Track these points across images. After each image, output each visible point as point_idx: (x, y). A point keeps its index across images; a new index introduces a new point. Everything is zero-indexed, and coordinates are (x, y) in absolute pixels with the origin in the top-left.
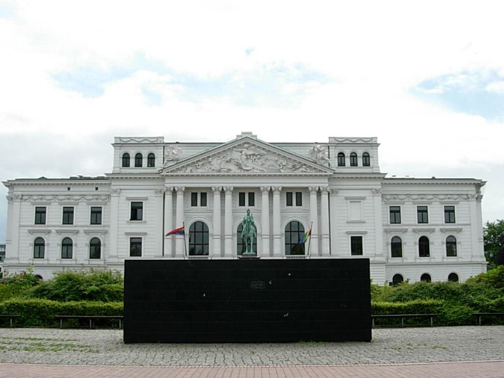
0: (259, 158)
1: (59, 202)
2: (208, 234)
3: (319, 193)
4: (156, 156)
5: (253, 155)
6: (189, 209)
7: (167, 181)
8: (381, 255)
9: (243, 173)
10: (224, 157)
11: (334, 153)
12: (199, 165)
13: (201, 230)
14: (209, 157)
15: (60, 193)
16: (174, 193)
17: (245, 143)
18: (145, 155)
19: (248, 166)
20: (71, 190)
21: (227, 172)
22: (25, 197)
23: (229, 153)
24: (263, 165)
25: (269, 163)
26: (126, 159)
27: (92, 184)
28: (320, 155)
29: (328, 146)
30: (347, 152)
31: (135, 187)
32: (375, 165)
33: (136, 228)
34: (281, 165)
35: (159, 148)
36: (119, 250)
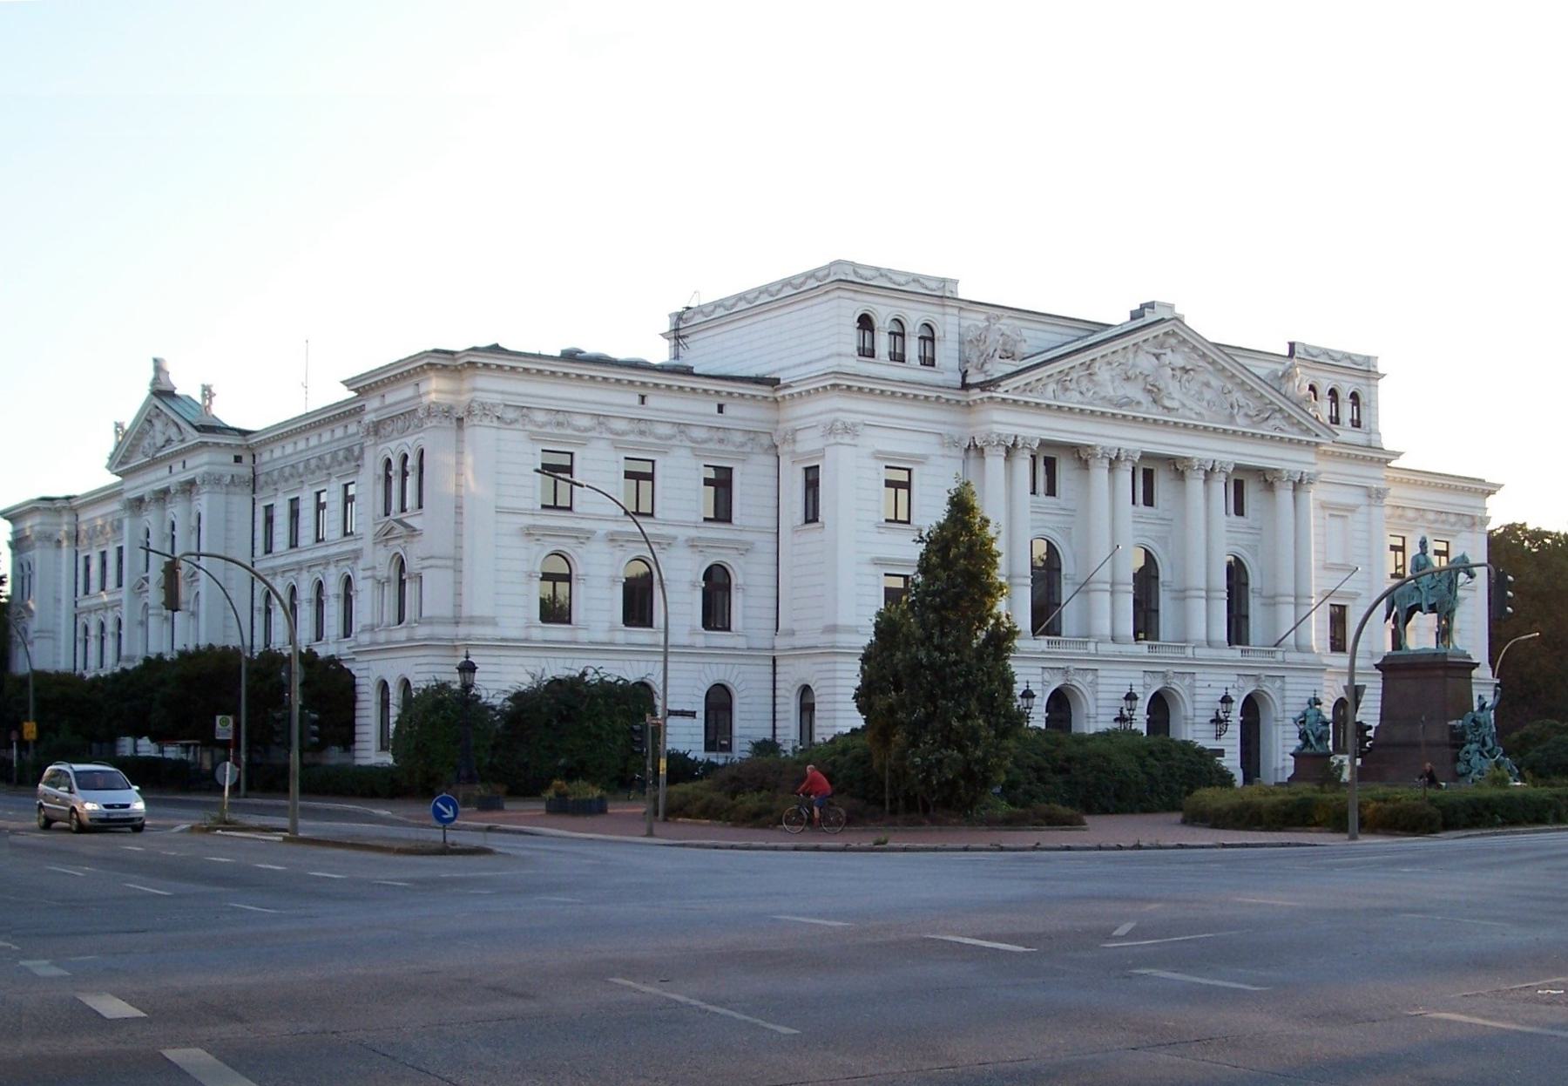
1: (613, 441)
9: (1156, 413)
18: (913, 329)
20: (650, 401)
35: (949, 310)
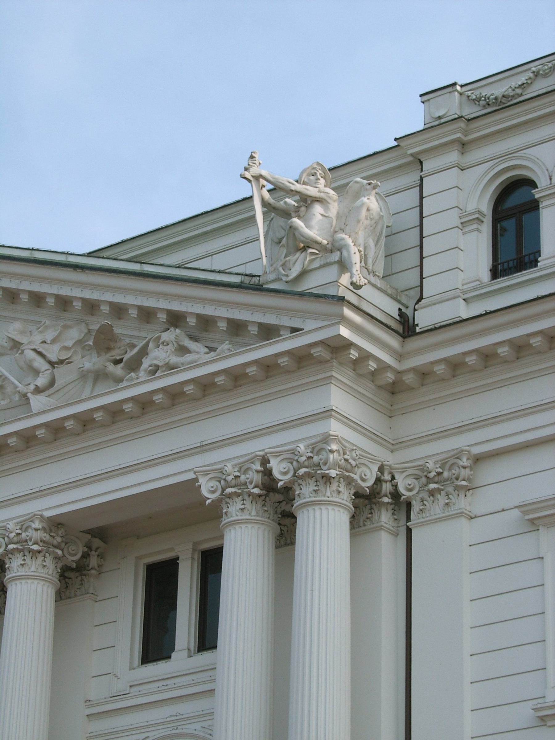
11: (461, 192)
29: (406, 159)
34: (40, 363)
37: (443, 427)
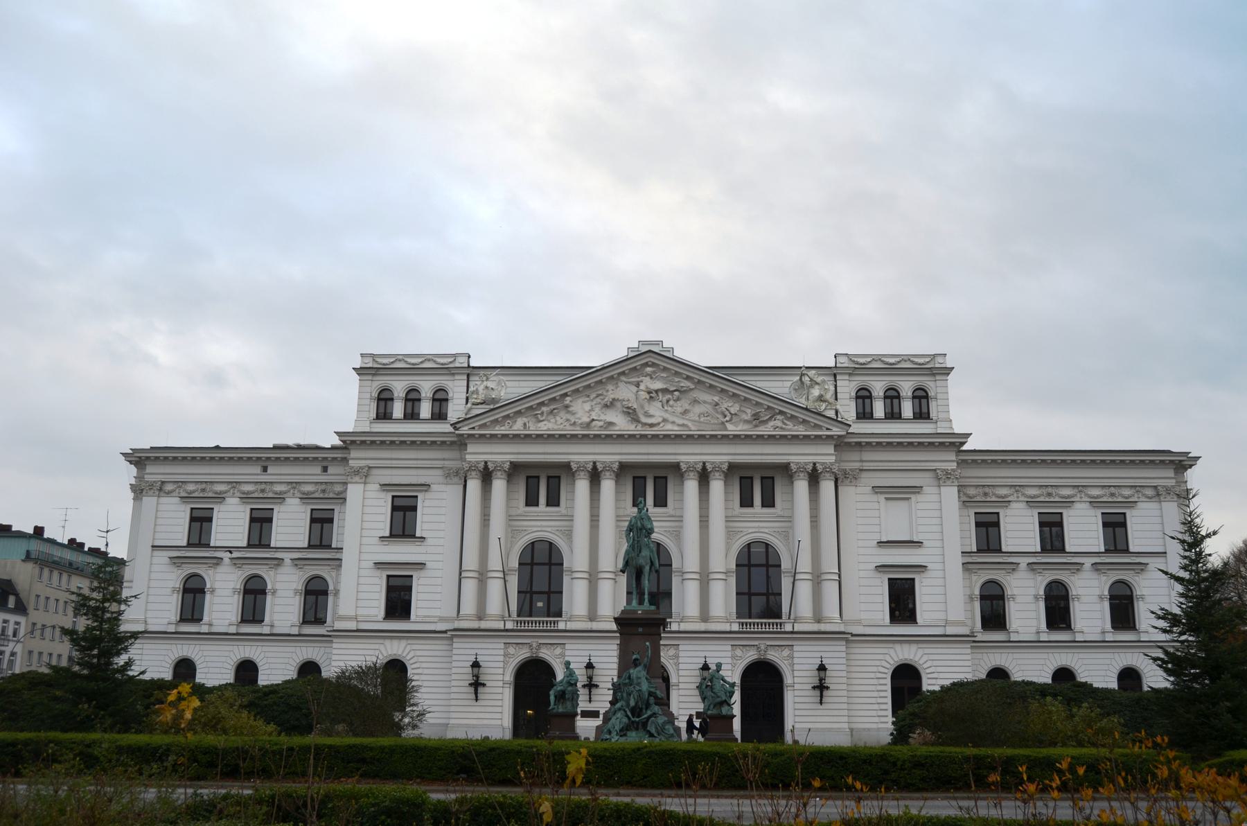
0: (678, 399)
2: (562, 571)
3: (814, 478)
4: (450, 395)
5: (665, 391)
6: (519, 512)
7: (470, 448)
8: (962, 624)
10: (598, 396)
11: (847, 388)
12: (542, 413)
13: (535, 567)
14: (566, 395)
15: (307, 479)
16: (487, 476)
17: (646, 365)
19: (651, 416)
20: (269, 471)
21: (606, 429)
22: (169, 487)
23: (610, 387)
24: (685, 412)
25: (698, 409)
26: (384, 400)
27: (316, 459)
28: (816, 392)
29: (833, 373)
30: (878, 387)
31: (420, 464)
32: (941, 416)
33: (402, 552)
35: (457, 377)
36: (361, 603)
37: (852, 461)
